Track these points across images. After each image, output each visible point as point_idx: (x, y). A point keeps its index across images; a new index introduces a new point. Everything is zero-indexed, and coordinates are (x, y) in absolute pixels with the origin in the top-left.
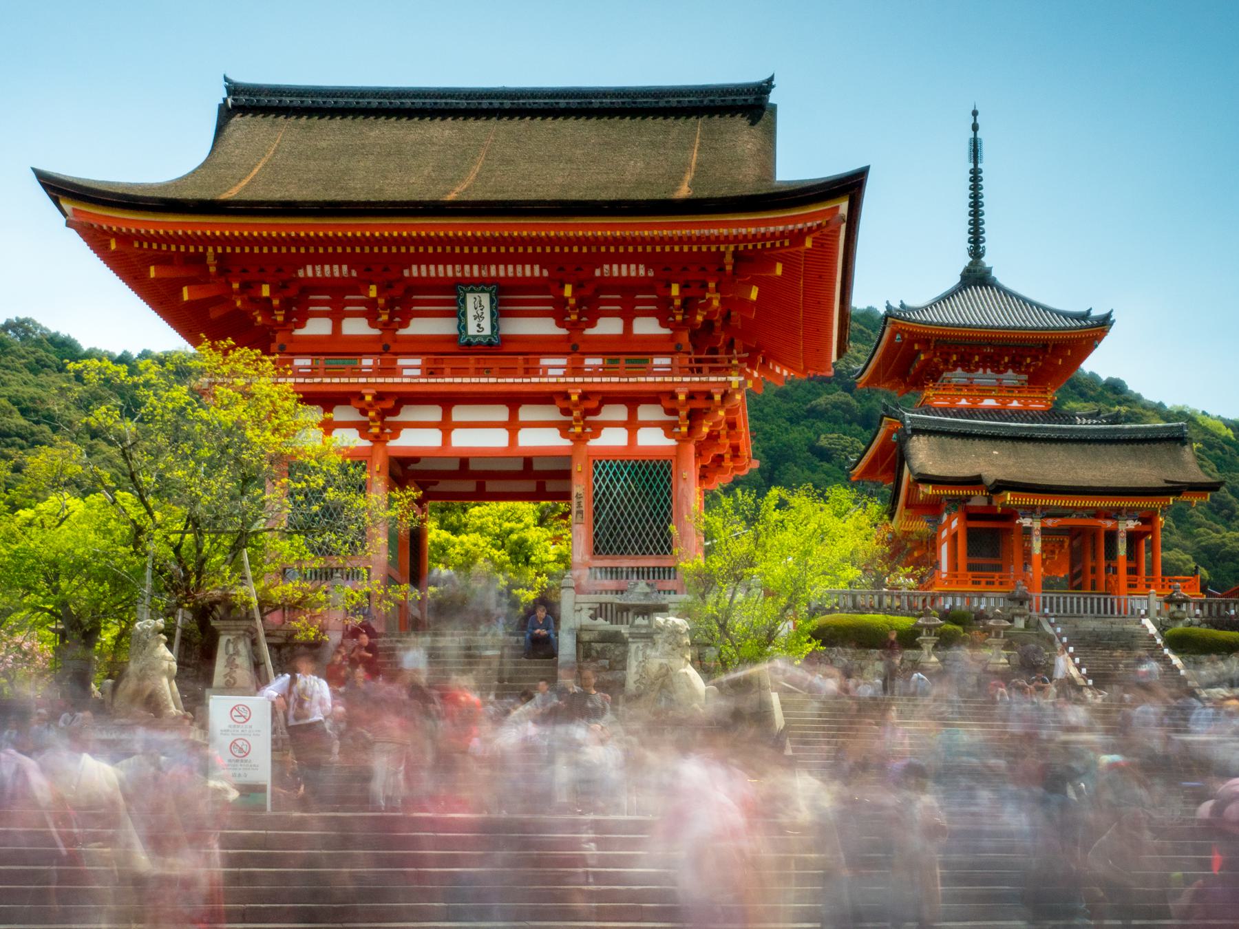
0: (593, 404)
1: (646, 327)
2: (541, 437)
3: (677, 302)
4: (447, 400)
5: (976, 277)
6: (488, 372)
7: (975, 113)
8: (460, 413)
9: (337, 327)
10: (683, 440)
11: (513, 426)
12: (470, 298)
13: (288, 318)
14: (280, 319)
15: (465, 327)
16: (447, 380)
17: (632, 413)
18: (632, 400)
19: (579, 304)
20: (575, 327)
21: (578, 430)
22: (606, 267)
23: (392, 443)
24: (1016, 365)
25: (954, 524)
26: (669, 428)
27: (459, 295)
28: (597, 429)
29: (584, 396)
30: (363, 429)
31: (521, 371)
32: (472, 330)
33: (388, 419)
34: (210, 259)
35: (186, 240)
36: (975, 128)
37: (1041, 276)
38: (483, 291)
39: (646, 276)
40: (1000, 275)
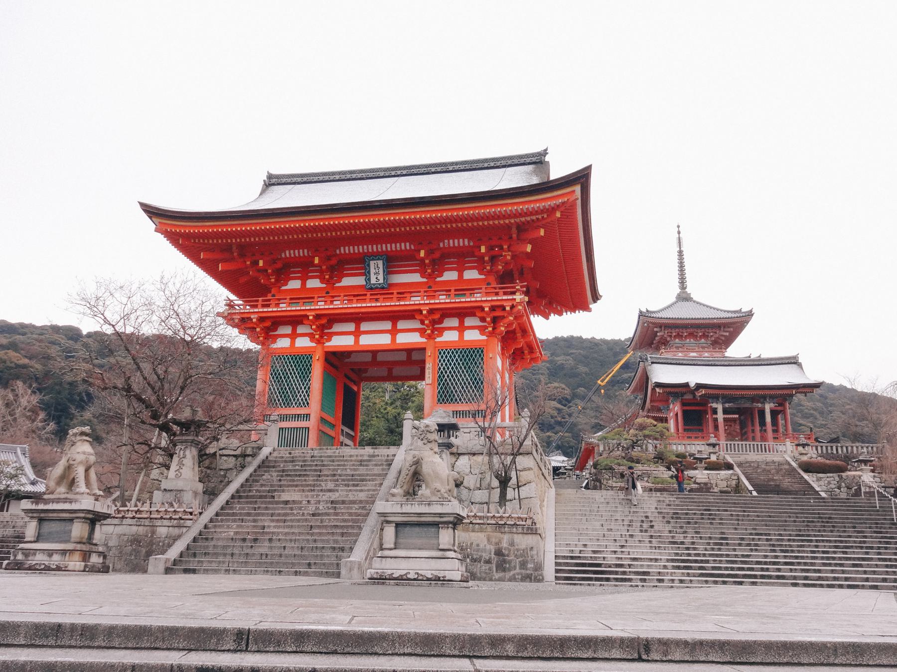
0: (437, 316)
1: (471, 274)
2: (409, 338)
3: (486, 258)
4: (357, 318)
5: (684, 297)
6: (377, 300)
7: (678, 227)
8: (365, 326)
9: (304, 284)
10: (491, 334)
11: (394, 332)
12: (372, 263)
13: (277, 280)
14: (273, 280)
15: (369, 279)
16: (354, 305)
17: (462, 322)
18: (461, 313)
19: (433, 262)
20: (431, 277)
21: (429, 332)
22: (446, 241)
23: (327, 344)
24: (705, 336)
25: (676, 409)
26: (482, 330)
27: (363, 262)
28: (441, 331)
29: (431, 311)
30: (311, 336)
31: (395, 299)
32: (373, 281)
33: (326, 331)
34: (234, 248)
35: (217, 235)
36: (679, 233)
37: (714, 297)
38: (379, 259)
39: (469, 246)
40: (695, 296)
